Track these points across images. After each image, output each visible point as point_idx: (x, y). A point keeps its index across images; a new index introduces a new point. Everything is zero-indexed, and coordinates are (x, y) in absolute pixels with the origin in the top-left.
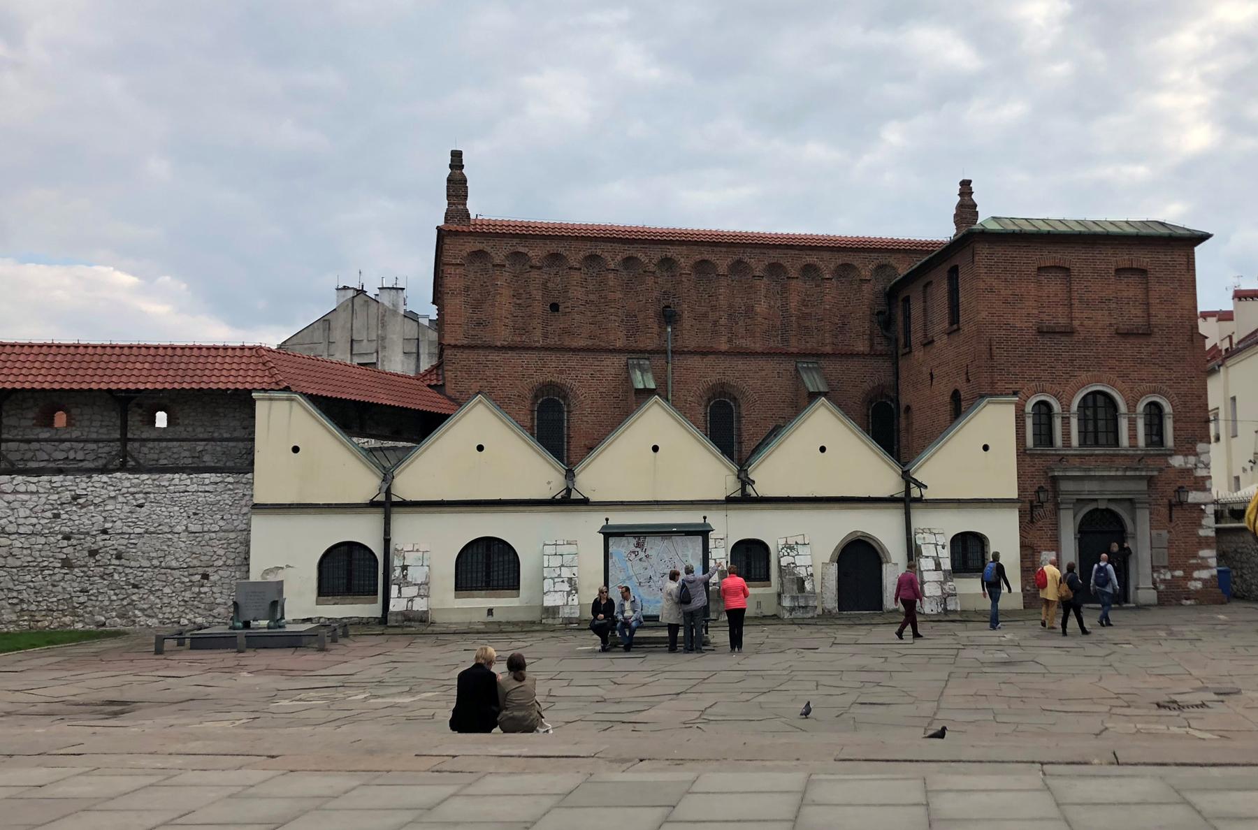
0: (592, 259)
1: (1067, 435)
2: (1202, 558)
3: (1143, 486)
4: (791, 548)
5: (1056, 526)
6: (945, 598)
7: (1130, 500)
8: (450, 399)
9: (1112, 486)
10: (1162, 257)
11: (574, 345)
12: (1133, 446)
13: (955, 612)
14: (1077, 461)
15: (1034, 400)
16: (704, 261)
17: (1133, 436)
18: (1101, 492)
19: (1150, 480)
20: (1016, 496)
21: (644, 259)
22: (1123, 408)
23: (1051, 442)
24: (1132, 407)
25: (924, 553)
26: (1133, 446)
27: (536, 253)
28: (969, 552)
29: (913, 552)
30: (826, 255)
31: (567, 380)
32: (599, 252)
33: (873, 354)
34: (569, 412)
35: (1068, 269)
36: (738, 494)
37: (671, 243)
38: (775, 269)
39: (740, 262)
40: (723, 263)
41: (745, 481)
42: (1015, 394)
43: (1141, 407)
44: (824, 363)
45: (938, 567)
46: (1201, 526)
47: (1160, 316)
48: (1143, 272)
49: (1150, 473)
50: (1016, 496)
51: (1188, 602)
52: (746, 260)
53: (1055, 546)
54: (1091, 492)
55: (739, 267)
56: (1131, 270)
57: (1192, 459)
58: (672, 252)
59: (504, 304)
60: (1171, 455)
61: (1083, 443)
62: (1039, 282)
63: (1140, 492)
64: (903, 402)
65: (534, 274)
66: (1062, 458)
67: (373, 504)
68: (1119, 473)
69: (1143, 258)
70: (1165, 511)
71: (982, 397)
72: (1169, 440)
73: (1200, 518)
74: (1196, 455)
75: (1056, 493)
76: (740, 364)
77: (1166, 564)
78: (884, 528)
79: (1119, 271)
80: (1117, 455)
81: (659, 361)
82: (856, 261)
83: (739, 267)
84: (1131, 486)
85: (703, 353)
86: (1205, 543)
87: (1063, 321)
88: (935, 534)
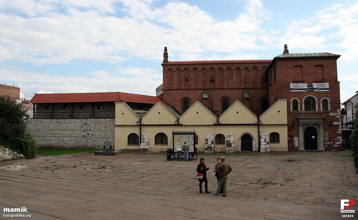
0: (195, 69)
3: (322, 121)
4: (229, 136)
8: (164, 101)
10: (327, 62)
11: (191, 88)
12: (319, 110)
16: (220, 68)
17: (319, 108)
18: (310, 122)
19: (324, 119)
20: (287, 123)
21: (206, 68)
22: (316, 101)
24: (319, 100)
26: (319, 110)
27: (182, 68)
28: (274, 137)
29: (259, 137)
30: (250, 65)
31: (189, 96)
32: (196, 67)
33: (262, 88)
34: (190, 104)
35: (302, 66)
36: (217, 123)
37: (212, 64)
38: (238, 68)
39: (229, 67)
40: (225, 68)
41: (218, 120)
42: (287, 98)
43: (321, 101)
44: (250, 90)
45: (265, 141)
46: (338, 131)
47: (327, 77)
48: (322, 66)
50: (286, 123)
51: (334, 150)
52: (231, 67)
53: (298, 135)
54: (307, 122)
55: (229, 68)
56: (319, 66)
57: (335, 114)
58: (213, 66)
59: (175, 79)
60: (330, 113)
61: (306, 109)
62: (294, 70)
64: (269, 99)
65: (182, 73)
66: (300, 114)
67: (138, 125)
69: (322, 62)
71: (279, 99)
72: (329, 109)
74: (337, 112)
75: (298, 123)
76: (229, 91)
78: (253, 132)
79: (315, 66)
81: (210, 91)
82: (258, 65)
83: (229, 68)
84: (318, 121)
85: (221, 89)
86: (339, 135)
87: (301, 79)
88: (266, 133)
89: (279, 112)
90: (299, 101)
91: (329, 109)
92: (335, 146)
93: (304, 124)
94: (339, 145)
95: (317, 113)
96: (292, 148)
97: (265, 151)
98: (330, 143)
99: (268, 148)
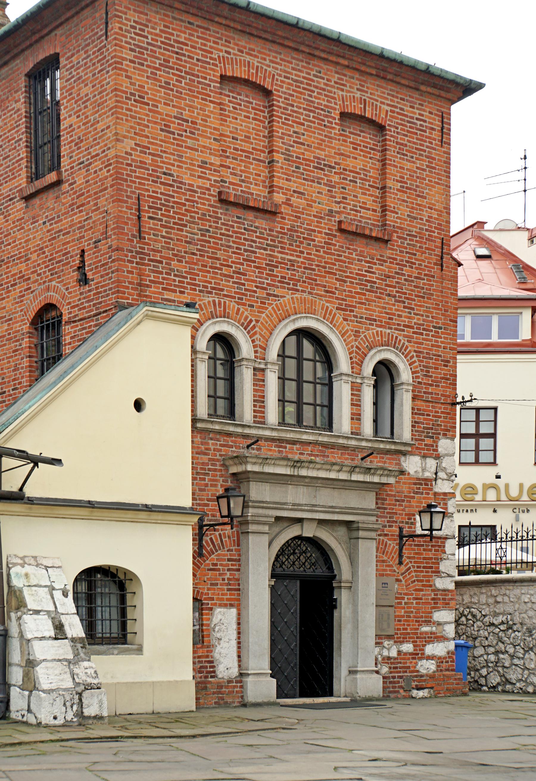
1: (260, 401)
2: (439, 624)
5: (238, 563)
6: (82, 690)
7: (348, 524)
9: (327, 498)
13: (99, 718)
14: (274, 451)
15: (211, 329)
18: (313, 507)
22: (343, 364)
23: (231, 413)
24: (357, 364)
25: (31, 604)
45: (59, 629)
49: (384, 480)
51: (421, 694)
53: (236, 598)
54: (296, 507)
63: (365, 512)
68: (343, 476)
70: (393, 545)
73: (438, 561)
77: (391, 632)
80: (333, 446)
89: (138, 405)
90: (245, 348)
91: (405, 432)
92: (427, 667)
93: (278, 519)
94: (440, 660)
95: (345, 448)
96: (213, 690)
97: (70, 716)
98: (399, 653)
99: (89, 687)
